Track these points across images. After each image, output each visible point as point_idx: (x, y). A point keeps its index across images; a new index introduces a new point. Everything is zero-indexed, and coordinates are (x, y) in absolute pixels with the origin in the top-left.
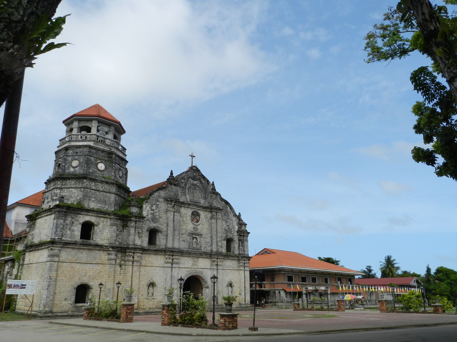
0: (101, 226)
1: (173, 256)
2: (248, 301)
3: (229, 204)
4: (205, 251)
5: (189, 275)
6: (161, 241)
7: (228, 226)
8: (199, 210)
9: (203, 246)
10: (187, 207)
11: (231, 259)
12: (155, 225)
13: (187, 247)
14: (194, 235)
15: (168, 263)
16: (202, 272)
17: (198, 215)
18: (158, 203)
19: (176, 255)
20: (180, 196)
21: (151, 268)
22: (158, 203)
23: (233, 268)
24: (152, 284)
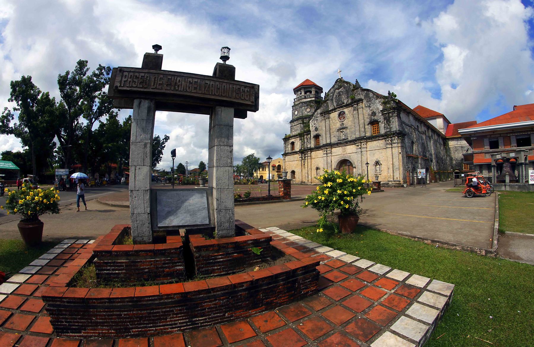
0: (296, 142)
1: (327, 149)
2: (397, 178)
3: (370, 90)
4: (351, 139)
5: (339, 160)
6: (323, 141)
7: (371, 110)
8: (343, 109)
9: (349, 136)
10: (335, 112)
11: (377, 140)
12: (317, 133)
13: (337, 140)
14: (342, 129)
15: (324, 154)
16: (350, 156)
17: (344, 113)
18: (317, 119)
19: (328, 148)
20: (329, 107)
21: (317, 159)
22: (317, 119)
23: (380, 147)
24: (317, 169)
